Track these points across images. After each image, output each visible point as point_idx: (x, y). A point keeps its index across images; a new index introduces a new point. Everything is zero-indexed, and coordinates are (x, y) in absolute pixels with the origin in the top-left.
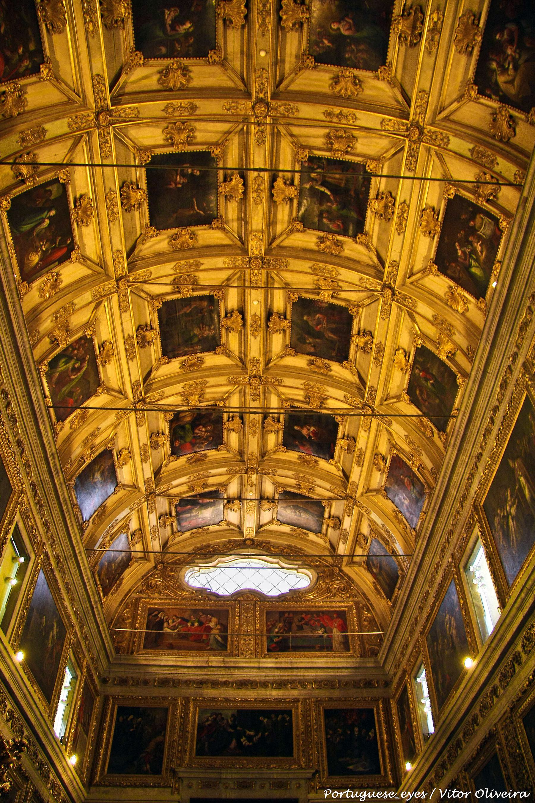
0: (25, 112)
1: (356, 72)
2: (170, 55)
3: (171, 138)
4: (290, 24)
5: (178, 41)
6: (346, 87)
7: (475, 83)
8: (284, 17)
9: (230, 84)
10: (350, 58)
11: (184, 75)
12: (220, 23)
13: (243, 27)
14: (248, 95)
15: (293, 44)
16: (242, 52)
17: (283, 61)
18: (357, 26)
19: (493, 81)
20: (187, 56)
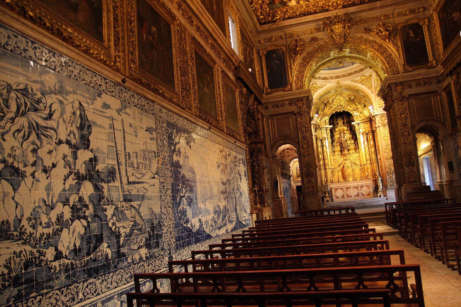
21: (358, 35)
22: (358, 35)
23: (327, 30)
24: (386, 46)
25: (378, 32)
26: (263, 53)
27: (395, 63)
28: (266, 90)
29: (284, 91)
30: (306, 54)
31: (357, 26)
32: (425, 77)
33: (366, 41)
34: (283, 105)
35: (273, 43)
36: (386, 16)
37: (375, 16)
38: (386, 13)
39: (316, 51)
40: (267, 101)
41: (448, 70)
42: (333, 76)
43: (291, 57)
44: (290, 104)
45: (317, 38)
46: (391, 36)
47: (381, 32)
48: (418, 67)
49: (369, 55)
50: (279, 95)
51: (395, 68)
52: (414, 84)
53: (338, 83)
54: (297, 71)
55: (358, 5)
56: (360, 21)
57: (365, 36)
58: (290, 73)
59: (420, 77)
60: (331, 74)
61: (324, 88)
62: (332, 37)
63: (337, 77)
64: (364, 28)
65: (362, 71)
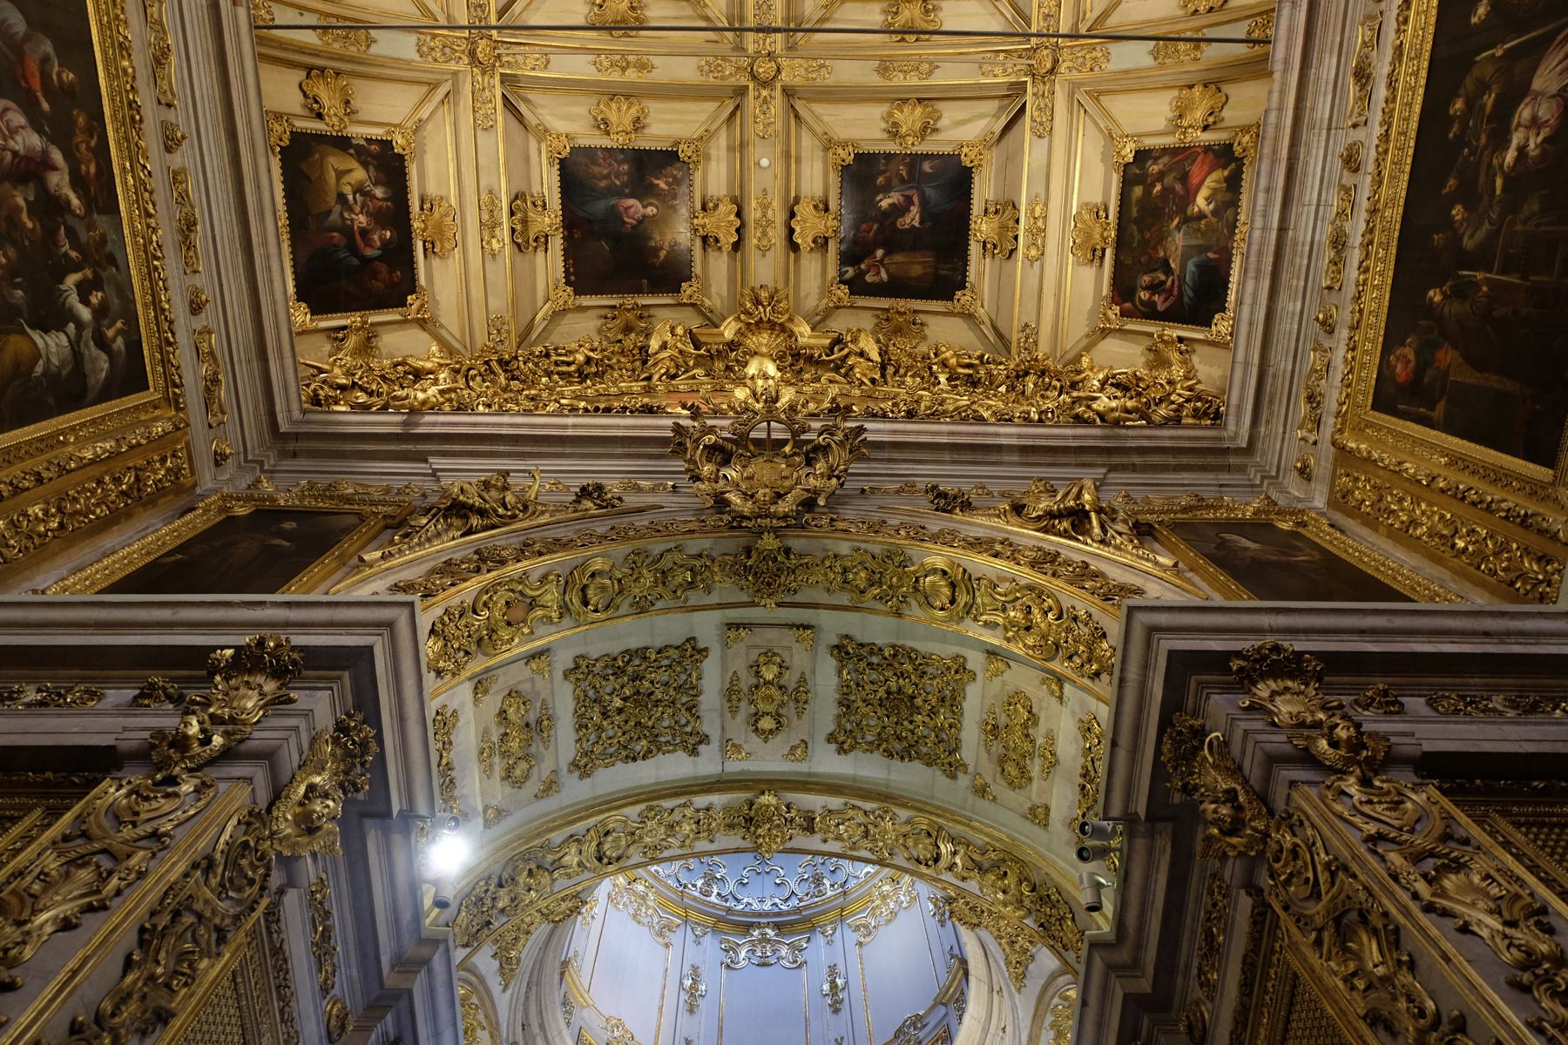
0: (1181, 88)
1: (605, 142)
2: (916, 159)
3: (927, 11)
4: (722, 208)
5: (902, 181)
6: (621, 115)
7: (401, 158)
8: (732, 217)
9: (818, 108)
10: (620, 163)
11: (895, 124)
12: (833, 206)
13: (797, 200)
14: (788, 92)
15: (714, 177)
16: (798, 161)
17: (731, 149)
18: (615, 215)
19: (371, 168)
20: (889, 157)
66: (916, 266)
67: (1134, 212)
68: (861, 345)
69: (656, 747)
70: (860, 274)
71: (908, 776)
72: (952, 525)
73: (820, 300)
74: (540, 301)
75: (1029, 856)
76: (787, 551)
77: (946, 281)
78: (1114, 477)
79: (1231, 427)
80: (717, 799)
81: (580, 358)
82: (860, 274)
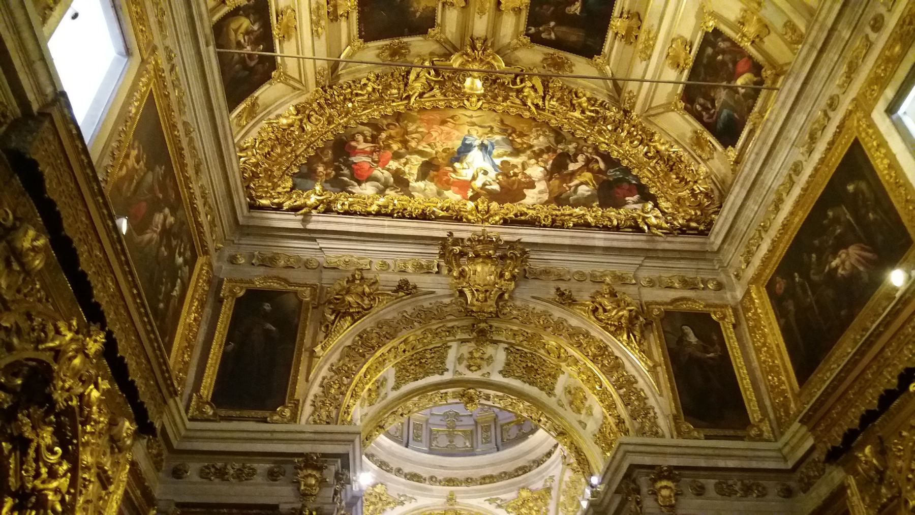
21: (539, 307)
22: (539, 307)
23: (450, 271)
24: (617, 353)
25: (595, 310)
26: (231, 291)
27: (647, 410)
28: (199, 408)
29: (264, 421)
30: (372, 324)
31: (537, 283)
32: (746, 464)
33: (559, 327)
34: (243, 475)
35: (274, 272)
36: (621, 279)
37: (587, 269)
38: (618, 270)
39: (408, 322)
40: (188, 446)
41: (837, 437)
42: (441, 474)
43: (323, 321)
44: (272, 475)
45: (415, 287)
46: (637, 324)
47: (605, 311)
48: (721, 432)
49: (561, 383)
50: (244, 432)
51: (648, 424)
52: (710, 484)
53: (451, 499)
54: (331, 369)
55: (545, 226)
56: (546, 272)
57: (557, 313)
58: (303, 368)
59: (731, 464)
60: (435, 466)
61: (408, 506)
62: (462, 293)
63: (450, 482)
64: (558, 289)
65: (525, 472)
66: (574, 36)
67: (705, 61)
68: (534, 82)
69: (427, 374)
70: (539, 33)
71: (534, 391)
72: (564, 316)
73: (512, 39)
74: (343, 48)
75: (576, 437)
76: (491, 326)
77: (591, 49)
78: (648, 263)
79: (712, 238)
80: (450, 390)
81: (370, 89)
82: (538, 33)
